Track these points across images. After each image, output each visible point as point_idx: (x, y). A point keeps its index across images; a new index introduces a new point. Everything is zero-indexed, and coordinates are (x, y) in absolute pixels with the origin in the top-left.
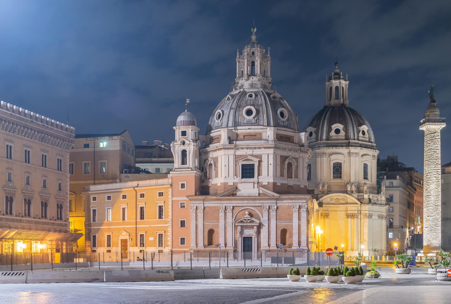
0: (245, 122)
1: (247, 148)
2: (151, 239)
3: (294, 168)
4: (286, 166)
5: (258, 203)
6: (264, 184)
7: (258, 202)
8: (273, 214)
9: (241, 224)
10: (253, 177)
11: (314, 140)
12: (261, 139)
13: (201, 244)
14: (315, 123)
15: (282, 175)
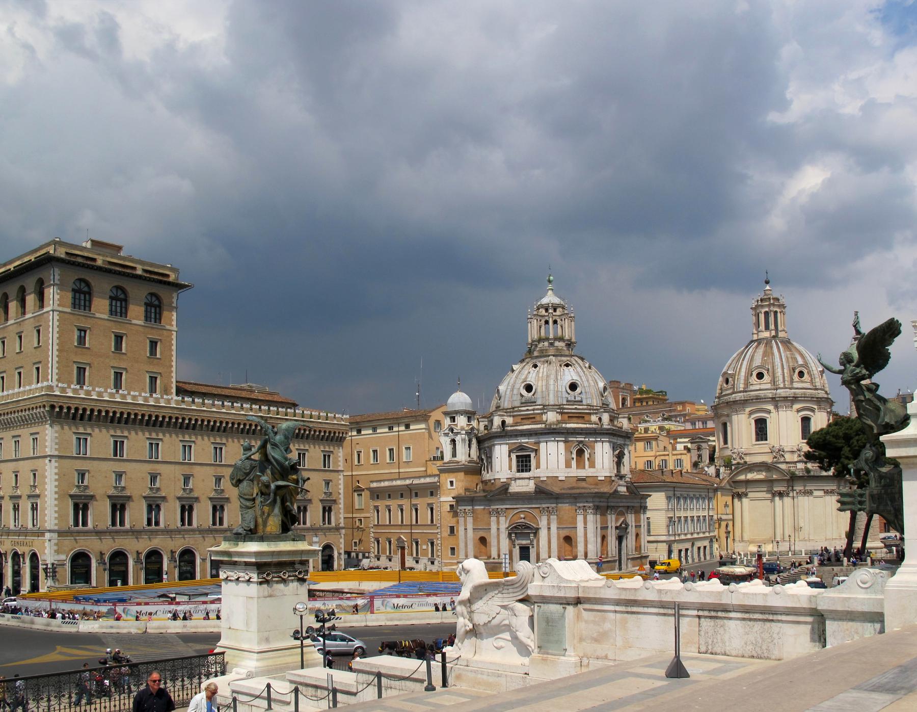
3: (587, 455)
4: (574, 456)
12: (541, 422)
14: (733, 366)
15: (568, 465)
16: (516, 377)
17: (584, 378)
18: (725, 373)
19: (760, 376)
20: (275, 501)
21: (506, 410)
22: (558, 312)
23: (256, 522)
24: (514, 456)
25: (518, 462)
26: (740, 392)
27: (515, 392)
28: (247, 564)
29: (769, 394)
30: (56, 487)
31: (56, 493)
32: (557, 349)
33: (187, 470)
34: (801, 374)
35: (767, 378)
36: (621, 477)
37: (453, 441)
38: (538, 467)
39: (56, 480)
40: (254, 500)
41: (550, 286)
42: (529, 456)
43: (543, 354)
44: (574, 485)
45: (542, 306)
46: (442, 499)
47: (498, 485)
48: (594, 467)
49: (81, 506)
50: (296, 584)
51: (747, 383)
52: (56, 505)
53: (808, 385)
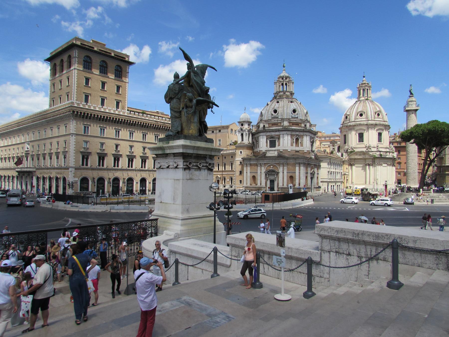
1: (272, 132)
2: (228, 180)
3: (300, 141)
4: (295, 141)
9: (269, 173)
10: (274, 146)
12: (281, 126)
15: (292, 145)
16: (270, 107)
17: (299, 108)
18: (346, 114)
19: (361, 115)
20: (195, 112)
21: (265, 121)
22: (287, 80)
23: (182, 127)
24: (268, 142)
27: (269, 113)
28: (175, 155)
29: (365, 123)
30: (74, 148)
31: (74, 150)
32: (287, 96)
33: (131, 144)
34: (378, 115)
35: (364, 116)
36: (313, 151)
37: (242, 135)
38: (279, 145)
39: (75, 145)
40: (180, 112)
41: (284, 69)
43: (281, 97)
44: (294, 154)
45: (281, 77)
47: (261, 153)
48: (302, 146)
49: (85, 156)
50: (206, 171)
51: (355, 118)
52: (74, 156)
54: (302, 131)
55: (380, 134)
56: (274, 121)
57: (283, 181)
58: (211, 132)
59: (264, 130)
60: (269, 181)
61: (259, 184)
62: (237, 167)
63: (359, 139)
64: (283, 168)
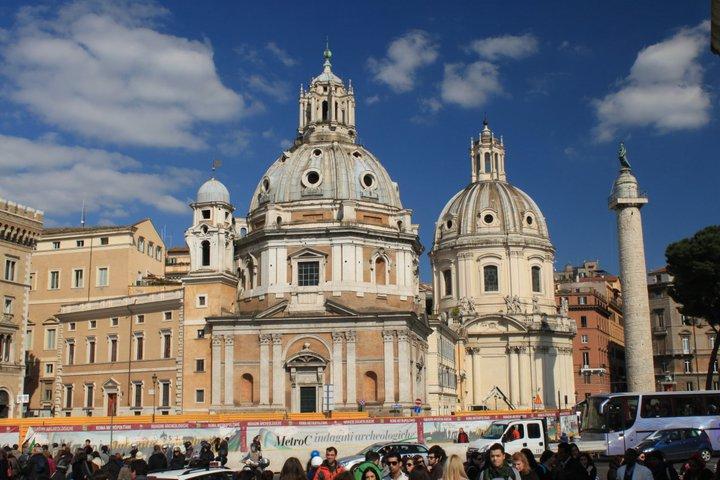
0: (306, 193)
3: (388, 268)
4: (374, 265)
5: (325, 327)
6: (334, 294)
7: (324, 325)
8: (351, 346)
11: (455, 234)
12: (328, 221)
13: (229, 400)
15: (367, 279)
19: (489, 219)
21: (282, 203)
24: (295, 264)
25: (300, 271)
26: (468, 235)
32: (339, 135)
34: (529, 220)
35: (496, 221)
38: (329, 278)
42: (318, 263)
46: (188, 322)
51: (475, 225)
53: (536, 232)
54: (392, 240)
55: (536, 269)
56: (310, 206)
57: (345, 388)
58: (75, 242)
59: (280, 234)
60: (298, 388)
61: (264, 398)
62: (191, 348)
63: (486, 283)
64: (344, 349)
